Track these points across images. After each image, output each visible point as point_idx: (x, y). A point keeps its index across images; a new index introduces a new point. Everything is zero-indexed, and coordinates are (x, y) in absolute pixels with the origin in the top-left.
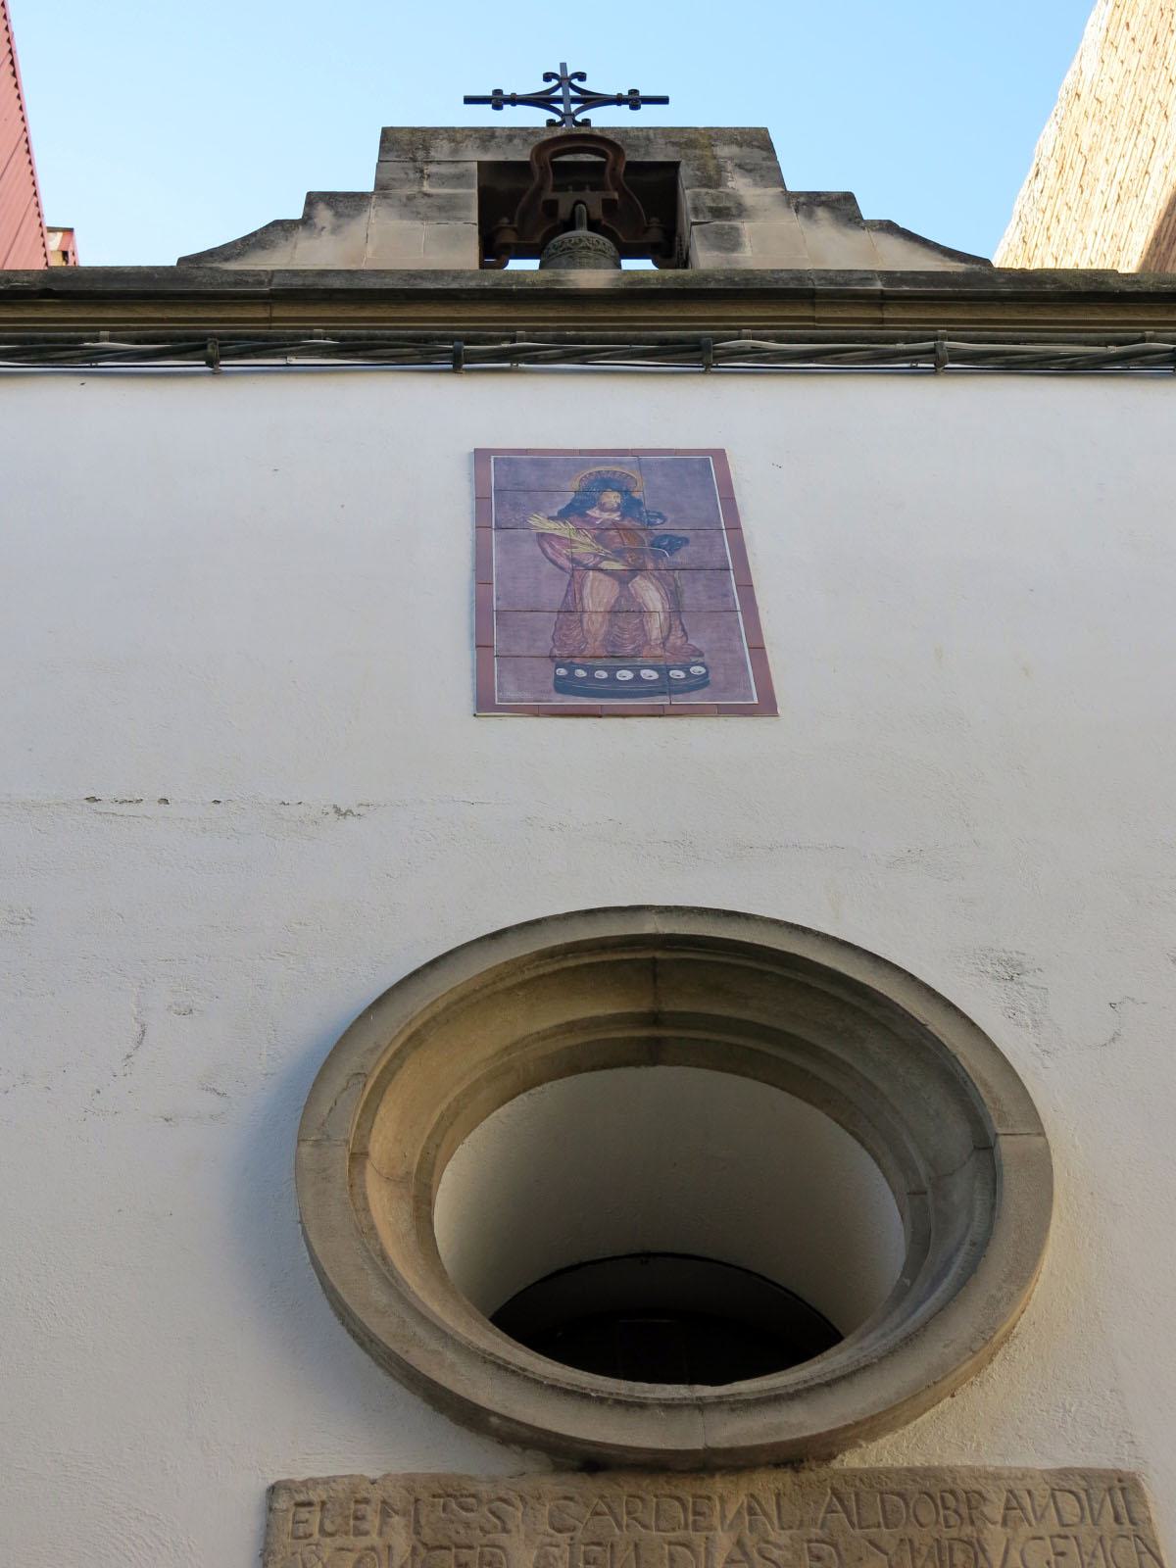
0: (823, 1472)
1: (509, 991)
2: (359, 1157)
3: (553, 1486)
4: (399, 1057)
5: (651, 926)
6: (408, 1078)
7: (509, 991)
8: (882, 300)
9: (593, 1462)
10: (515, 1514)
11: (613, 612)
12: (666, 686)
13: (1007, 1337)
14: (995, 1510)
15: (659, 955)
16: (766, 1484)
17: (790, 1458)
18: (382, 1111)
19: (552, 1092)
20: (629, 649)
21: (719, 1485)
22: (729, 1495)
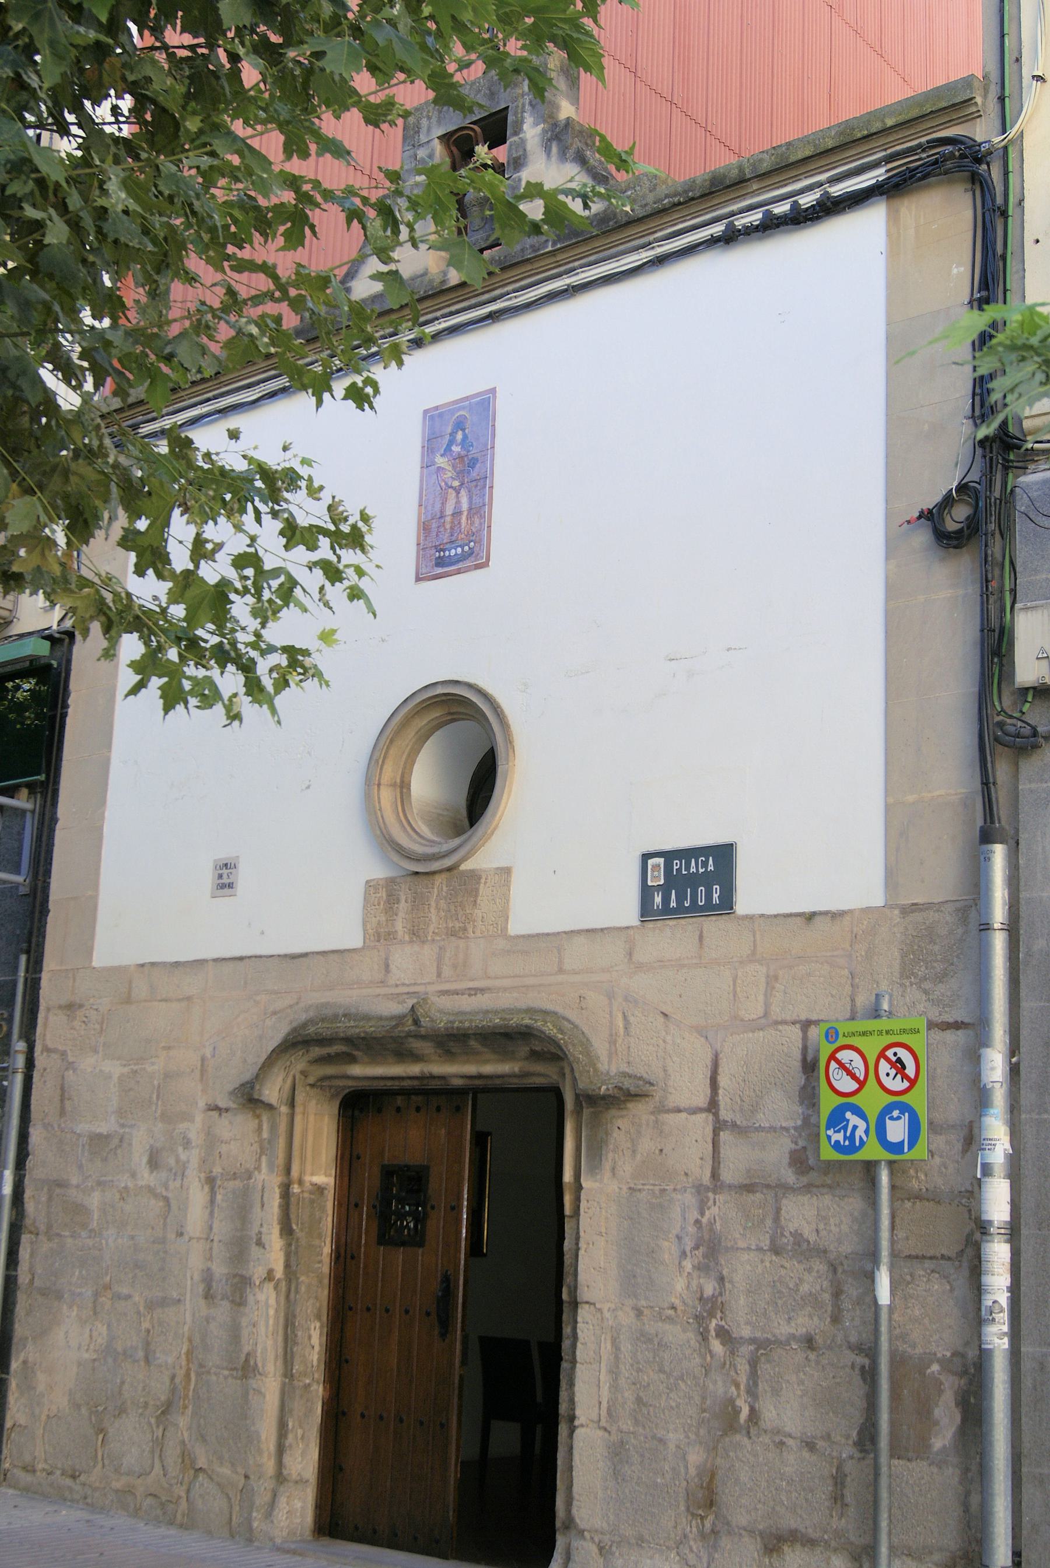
0: (455, 871)
1: (412, 717)
2: (379, 785)
3: (409, 879)
4: (388, 748)
5: (440, 690)
6: (393, 752)
7: (412, 717)
8: (552, 253)
9: (417, 873)
10: (403, 886)
11: (453, 515)
12: (464, 557)
13: (495, 829)
14: (483, 881)
15: (444, 698)
16: (444, 876)
17: (449, 869)
18: (385, 767)
19: (438, 734)
20: (454, 538)
21: (437, 877)
22: (439, 879)
